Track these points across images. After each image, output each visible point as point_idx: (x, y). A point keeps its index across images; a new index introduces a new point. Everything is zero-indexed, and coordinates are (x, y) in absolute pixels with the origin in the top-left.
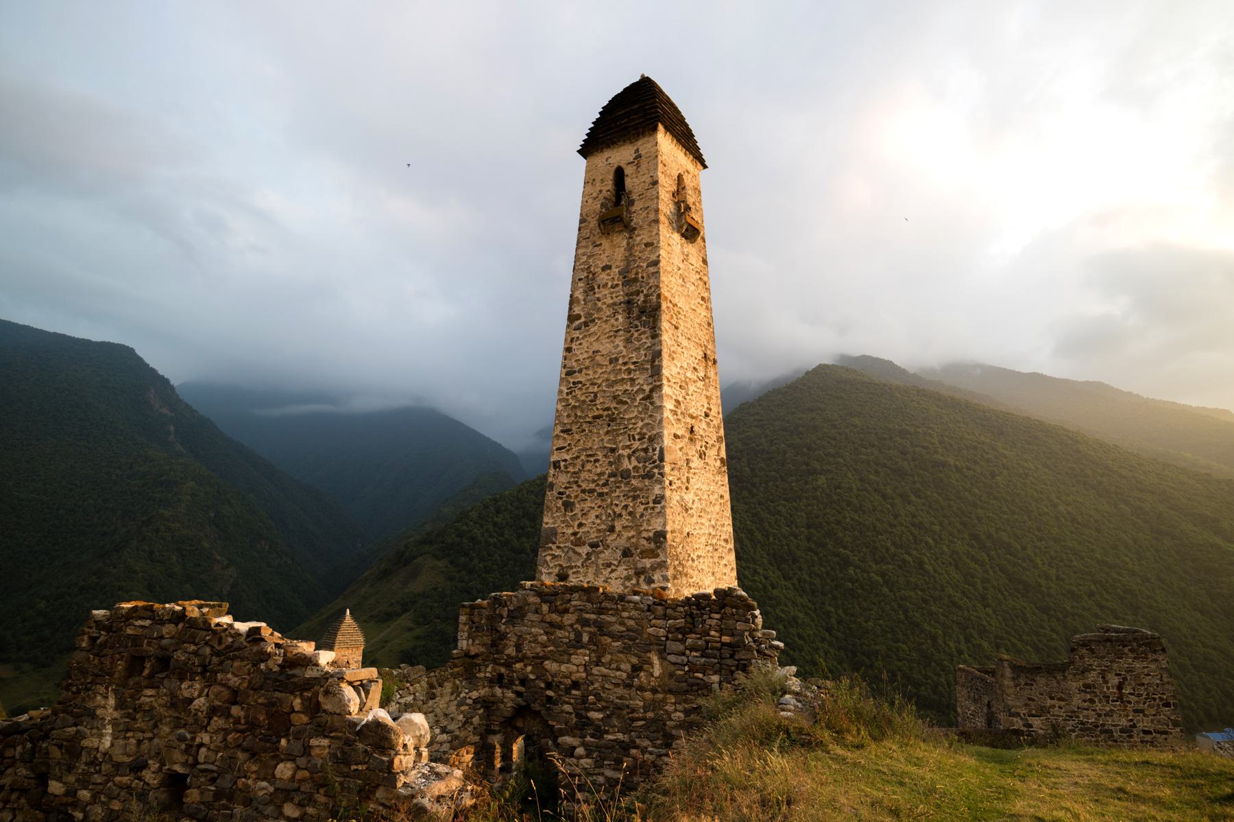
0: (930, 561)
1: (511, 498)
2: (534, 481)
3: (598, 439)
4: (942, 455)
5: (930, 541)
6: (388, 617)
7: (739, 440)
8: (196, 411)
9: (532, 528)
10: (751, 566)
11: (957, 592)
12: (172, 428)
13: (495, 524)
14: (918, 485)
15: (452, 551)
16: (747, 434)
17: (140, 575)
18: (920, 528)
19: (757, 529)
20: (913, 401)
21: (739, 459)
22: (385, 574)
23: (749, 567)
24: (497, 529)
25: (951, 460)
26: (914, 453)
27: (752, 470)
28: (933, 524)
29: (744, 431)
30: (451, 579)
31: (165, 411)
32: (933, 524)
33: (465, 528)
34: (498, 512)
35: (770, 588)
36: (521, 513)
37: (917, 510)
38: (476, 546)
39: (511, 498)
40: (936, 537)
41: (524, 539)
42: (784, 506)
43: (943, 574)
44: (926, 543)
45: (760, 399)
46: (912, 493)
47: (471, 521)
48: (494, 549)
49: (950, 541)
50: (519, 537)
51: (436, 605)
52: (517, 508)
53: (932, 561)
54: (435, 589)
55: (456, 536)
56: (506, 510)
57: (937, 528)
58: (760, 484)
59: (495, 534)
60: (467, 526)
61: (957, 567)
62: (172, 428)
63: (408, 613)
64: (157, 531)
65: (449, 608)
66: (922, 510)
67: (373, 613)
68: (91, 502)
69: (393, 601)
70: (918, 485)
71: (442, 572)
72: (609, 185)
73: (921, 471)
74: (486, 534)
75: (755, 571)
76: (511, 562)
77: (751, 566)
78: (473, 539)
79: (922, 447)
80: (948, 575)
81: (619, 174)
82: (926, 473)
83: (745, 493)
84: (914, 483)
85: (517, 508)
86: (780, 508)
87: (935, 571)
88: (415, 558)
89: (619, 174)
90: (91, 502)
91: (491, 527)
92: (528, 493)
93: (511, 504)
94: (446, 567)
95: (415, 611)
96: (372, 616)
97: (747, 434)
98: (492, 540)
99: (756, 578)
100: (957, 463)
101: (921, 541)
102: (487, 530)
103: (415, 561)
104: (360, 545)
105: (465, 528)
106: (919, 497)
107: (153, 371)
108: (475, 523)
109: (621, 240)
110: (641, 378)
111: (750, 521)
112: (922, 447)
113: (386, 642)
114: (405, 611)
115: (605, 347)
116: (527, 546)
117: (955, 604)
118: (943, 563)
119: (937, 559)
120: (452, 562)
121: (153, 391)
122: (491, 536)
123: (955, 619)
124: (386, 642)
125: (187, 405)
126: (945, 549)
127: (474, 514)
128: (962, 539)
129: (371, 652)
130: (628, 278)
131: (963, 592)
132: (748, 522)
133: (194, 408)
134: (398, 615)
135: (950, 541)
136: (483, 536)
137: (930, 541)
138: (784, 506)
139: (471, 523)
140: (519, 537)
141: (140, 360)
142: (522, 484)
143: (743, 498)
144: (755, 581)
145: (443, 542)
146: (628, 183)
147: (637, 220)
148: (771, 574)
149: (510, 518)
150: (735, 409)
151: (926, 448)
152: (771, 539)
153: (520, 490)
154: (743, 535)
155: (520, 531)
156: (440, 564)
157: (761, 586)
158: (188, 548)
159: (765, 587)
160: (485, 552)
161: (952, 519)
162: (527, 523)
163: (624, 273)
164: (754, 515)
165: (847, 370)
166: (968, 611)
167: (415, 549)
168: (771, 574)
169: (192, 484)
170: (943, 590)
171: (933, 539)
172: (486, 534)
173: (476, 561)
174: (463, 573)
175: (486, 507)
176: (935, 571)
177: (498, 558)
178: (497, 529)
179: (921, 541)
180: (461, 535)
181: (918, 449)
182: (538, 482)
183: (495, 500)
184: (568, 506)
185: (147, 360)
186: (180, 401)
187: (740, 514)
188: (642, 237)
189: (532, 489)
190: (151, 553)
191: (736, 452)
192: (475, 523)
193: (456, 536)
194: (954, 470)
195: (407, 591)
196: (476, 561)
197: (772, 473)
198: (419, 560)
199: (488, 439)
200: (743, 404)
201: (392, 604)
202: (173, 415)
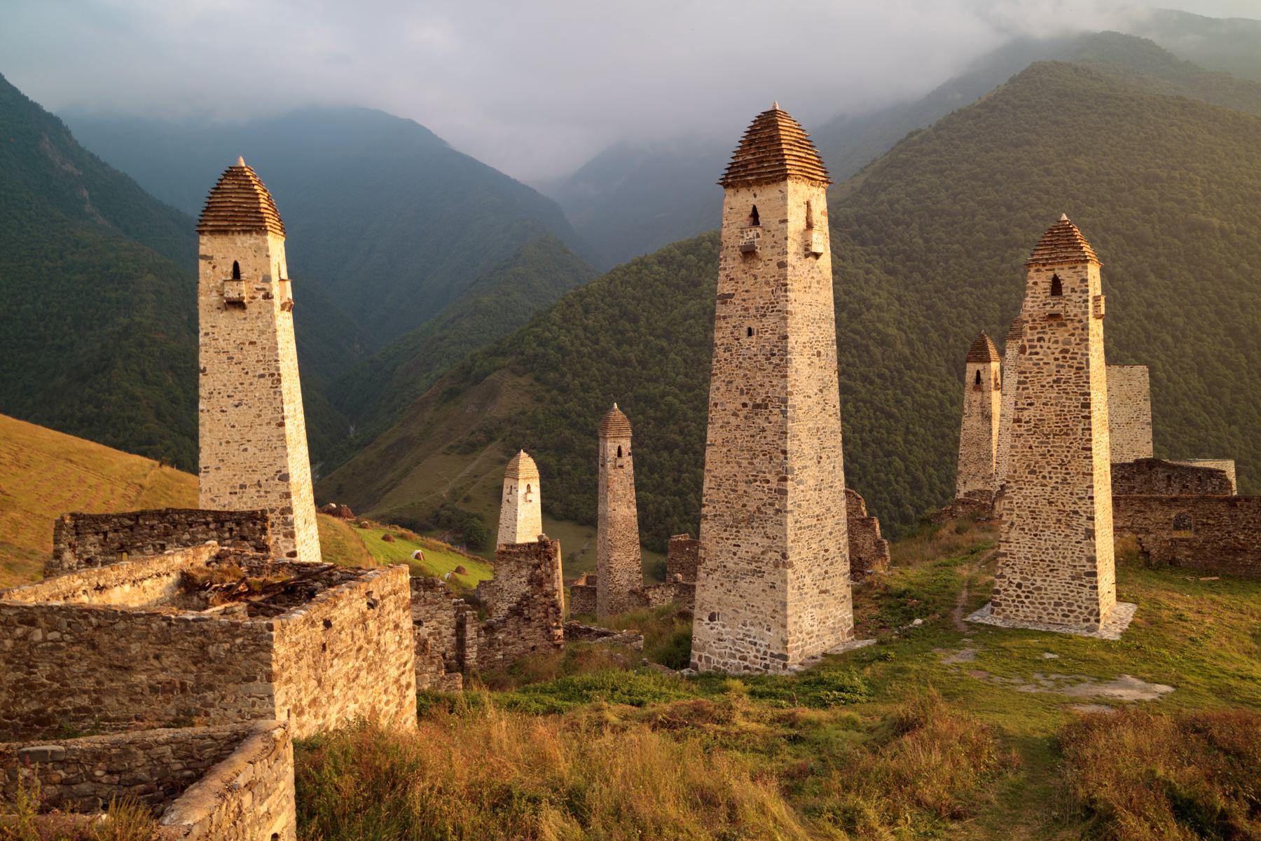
0: (1163, 366)
1: (602, 293)
2: (628, 267)
3: (974, 449)
4: (1204, 213)
5: (1169, 339)
6: (471, 448)
7: (908, 195)
8: (105, 165)
9: (634, 331)
10: (925, 376)
11: (1195, 406)
12: (86, 194)
13: (585, 329)
14: (1162, 259)
15: (535, 365)
16: (920, 185)
17: (144, 402)
18: (1156, 322)
19: (933, 326)
20: (1172, 125)
21: (908, 225)
22: (451, 395)
23: (922, 379)
24: (589, 335)
25: (1216, 222)
26: (1162, 210)
27: (927, 241)
28: (1176, 315)
29: (914, 181)
30: (539, 400)
31: (69, 167)
32: (1176, 315)
33: (547, 334)
34: (587, 311)
35: (948, 405)
36: (617, 312)
37: (1156, 297)
38: (567, 358)
39: (602, 293)
40: (1178, 333)
41: (626, 347)
42: (971, 294)
43: (1179, 383)
44: (1163, 342)
45: (938, 127)
46: (1152, 271)
47: (554, 324)
48: (590, 361)
49: (1196, 338)
50: (619, 344)
51: (528, 432)
52: (611, 306)
53: (1168, 367)
54: (523, 413)
55: (538, 346)
56: (596, 309)
57: (1180, 321)
58: (938, 263)
59: (587, 342)
60: (550, 331)
61: (1201, 373)
62: (86, 194)
63: (493, 444)
64: (141, 345)
65: (546, 436)
66: (1163, 296)
67: (452, 443)
68: (28, 306)
69: (474, 429)
70: (1162, 259)
71: (527, 392)
72: (975, 375)
73: (1169, 239)
74: (577, 343)
75: (930, 383)
76: (614, 377)
77: (925, 376)
78: (560, 349)
79: (1177, 201)
80: (1187, 383)
81: (978, 373)
82: (1176, 241)
83: (917, 276)
84: (1157, 256)
85: (611, 306)
86: (964, 297)
87: (1169, 379)
88: (487, 374)
89: (978, 373)
90: (28, 306)
91: (581, 333)
92: (622, 283)
93: (602, 301)
94: (531, 385)
95: (504, 440)
96: (451, 447)
97: (920, 185)
98: (585, 350)
99: (930, 392)
100: (1225, 224)
101: (1156, 339)
102: (577, 337)
103: (488, 378)
104: (358, 346)
105: (547, 334)
106: (1161, 277)
107: (35, 107)
108: (560, 328)
109: (980, 394)
110: (986, 435)
111: (923, 316)
112: (1177, 201)
113: (476, 476)
114: (492, 439)
115: (975, 424)
116: (632, 356)
117: (1190, 422)
118: (1182, 369)
119: (1175, 363)
120: (537, 379)
121: (47, 139)
122: (582, 345)
123: (1186, 440)
124: (476, 476)
125: (92, 156)
126: (1188, 350)
127: (556, 316)
128: (1214, 335)
129: (462, 488)
130: (982, 406)
131: (1204, 406)
132: (921, 318)
133: (103, 159)
134: (484, 445)
135: (1196, 338)
136: (573, 345)
137: (1169, 339)
138: (971, 294)
139: (555, 327)
140: (619, 344)
141: (14, 90)
142: (612, 272)
143: (914, 284)
144: (928, 396)
145: (522, 354)
146: (982, 376)
147: (984, 389)
148: (950, 386)
149: (604, 319)
150: (900, 142)
151: (1180, 202)
152: (951, 341)
153: (611, 281)
154: (914, 336)
155: (619, 336)
156: (525, 381)
157: (937, 403)
158: (182, 365)
159: (941, 404)
160: (578, 366)
161: (1205, 307)
162: (628, 326)
163: (981, 404)
164: (929, 308)
165: (1076, 70)
166: (1207, 430)
167: (485, 363)
168: (950, 386)
169: (150, 277)
170: (1177, 405)
171: (1174, 336)
172: (577, 343)
173: (569, 376)
174: (555, 392)
175: (570, 306)
176: (1169, 379)
177: (596, 372)
178: (589, 335)
179: (1156, 339)
180: (543, 343)
181: (1169, 204)
182: (634, 268)
183: (580, 295)
184: (965, 465)
185: (25, 90)
186: (82, 150)
187: (910, 307)
188: (986, 395)
189: (626, 278)
190: (143, 374)
191: (903, 214)
192: (560, 328)
193: (538, 346)
194: (1218, 235)
195: (487, 415)
196: (569, 376)
197: (955, 246)
198: (494, 376)
199: (516, 182)
200: (911, 134)
201: (473, 433)
202: (81, 173)
